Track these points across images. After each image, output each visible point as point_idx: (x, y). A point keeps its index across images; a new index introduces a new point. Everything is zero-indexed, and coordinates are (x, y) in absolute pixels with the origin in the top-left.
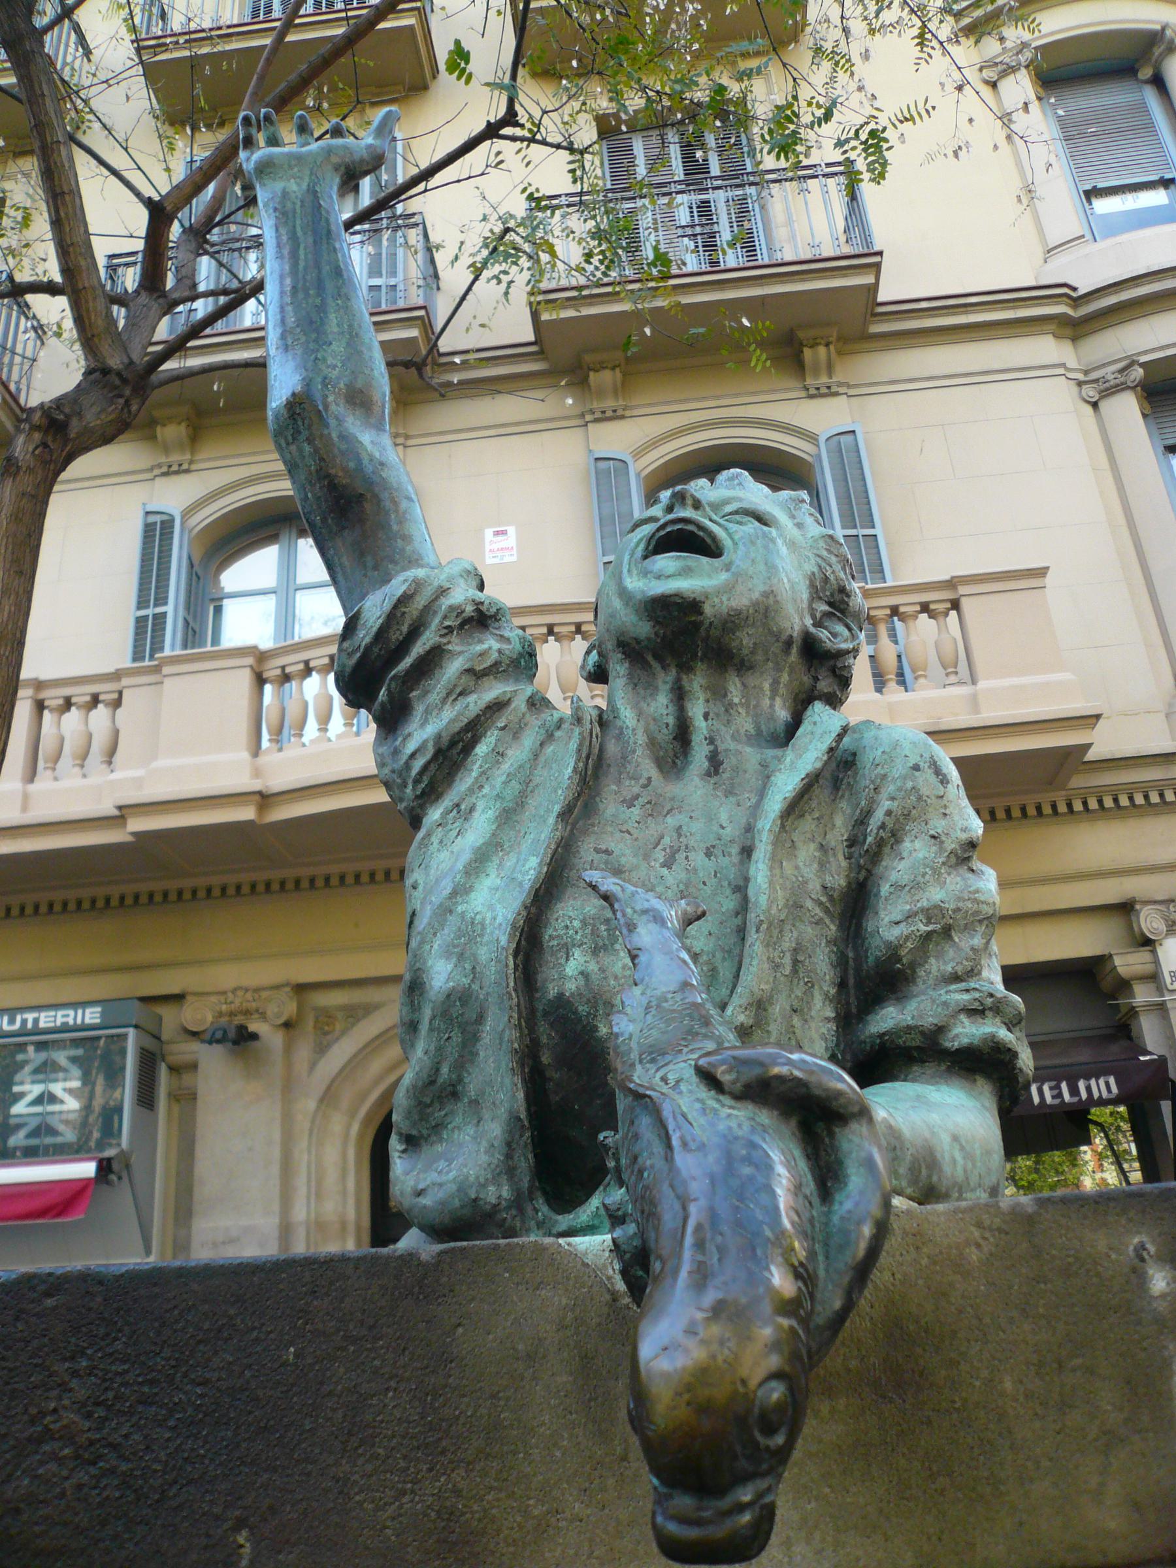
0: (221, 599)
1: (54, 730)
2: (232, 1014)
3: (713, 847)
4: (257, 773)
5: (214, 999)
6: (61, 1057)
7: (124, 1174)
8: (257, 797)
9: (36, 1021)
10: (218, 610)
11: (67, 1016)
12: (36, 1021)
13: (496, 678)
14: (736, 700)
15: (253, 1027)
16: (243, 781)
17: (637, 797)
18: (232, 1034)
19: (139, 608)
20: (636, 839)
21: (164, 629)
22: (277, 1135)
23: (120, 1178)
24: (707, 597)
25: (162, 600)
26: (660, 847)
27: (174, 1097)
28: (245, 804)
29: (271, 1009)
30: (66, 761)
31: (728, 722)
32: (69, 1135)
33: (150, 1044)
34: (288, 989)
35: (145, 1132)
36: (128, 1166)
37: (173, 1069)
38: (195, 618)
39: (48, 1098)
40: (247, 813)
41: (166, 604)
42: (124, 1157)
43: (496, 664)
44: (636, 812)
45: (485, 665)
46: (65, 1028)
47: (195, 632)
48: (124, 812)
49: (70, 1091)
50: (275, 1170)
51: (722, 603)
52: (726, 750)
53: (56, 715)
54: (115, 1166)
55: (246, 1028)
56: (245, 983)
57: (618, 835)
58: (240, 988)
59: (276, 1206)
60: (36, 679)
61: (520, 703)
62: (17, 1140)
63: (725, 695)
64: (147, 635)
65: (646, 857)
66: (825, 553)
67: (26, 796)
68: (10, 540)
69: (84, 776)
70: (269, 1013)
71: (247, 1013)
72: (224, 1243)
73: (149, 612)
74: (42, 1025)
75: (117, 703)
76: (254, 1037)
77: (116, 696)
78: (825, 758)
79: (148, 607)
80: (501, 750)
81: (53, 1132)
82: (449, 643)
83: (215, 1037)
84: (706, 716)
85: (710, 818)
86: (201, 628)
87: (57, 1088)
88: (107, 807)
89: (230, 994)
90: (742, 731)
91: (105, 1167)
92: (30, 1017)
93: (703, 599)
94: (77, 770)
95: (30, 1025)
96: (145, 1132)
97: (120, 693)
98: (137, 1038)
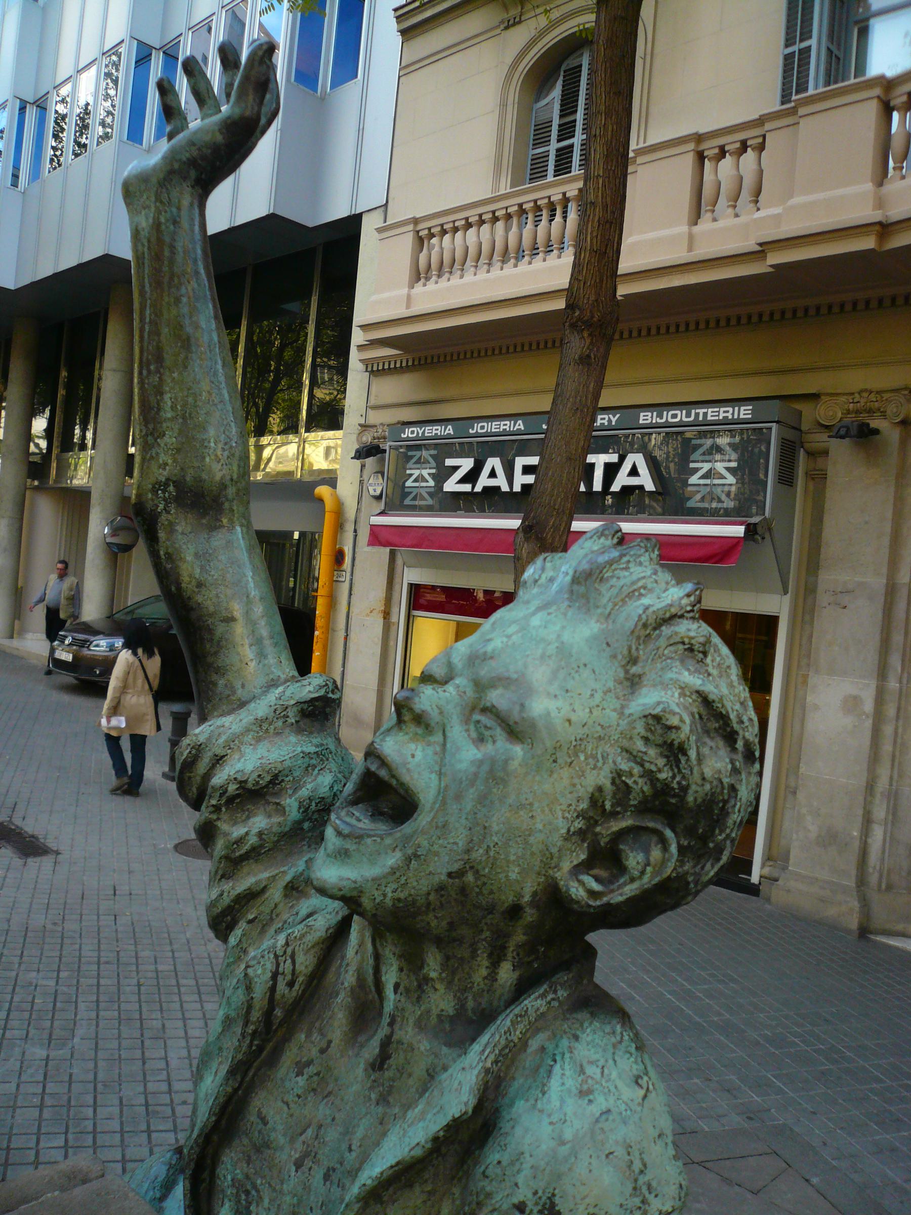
0: (868, 19)
1: (712, 177)
2: (858, 412)
3: (334, 1170)
4: (880, 203)
5: (843, 399)
7: (767, 536)
8: (877, 228)
9: (705, 414)
10: (864, 32)
11: (728, 412)
12: (705, 414)
13: (256, 861)
14: (433, 975)
15: (874, 424)
16: (866, 213)
17: (309, 1063)
18: (854, 431)
19: (787, 46)
20: (292, 1116)
21: (809, 63)
22: (889, 515)
23: (763, 538)
24: (361, 892)
25: (806, 35)
26: (303, 1137)
27: (810, 476)
28: (867, 234)
29: (891, 409)
30: (722, 201)
31: (419, 999)
32: (729, 504)
33: (790, 435)
34: (906, 392)
35: (785, 506)
36: (770, 529)
37: (810, 454)
38: (839, 45)
40: (868, 243)
41: (810, 37)
42: (767, 525)
43: (254, 849)
44: (301, 1081)
45: (242, 852)
47: (838, 58)
48: (765, 248)
49: (727, 469)
50: (886, 541)
51: (385, 895)
52: (400, 1042)
53: (713, 163)
54: (759, 529)
55: (868, 424)
56: (868, 387)
57: (280, 1104)
58: (866, 390)
59: (884, 570)
60: (696, 134)
61: (276, 894)
63: (421, 967)
64: (794, 70)
65: (292, 1140)
66: (640, 745)
67: (691, 237)
68: (608, 65)
69: (737, 216)
70: (889, 413)
71: (870, 411)
72: (841, 592)
73: (795, 48)
74: (709, 418)
75: (761, 147)
76: (876, 432)
77: (760, 140)
78: (429, 1146)
79: (794, 43)
80: (245, 946)
82: (218, 819)
83: (840, 432)
84: (396, 987)
85: (347, 1132)
86: (845, 56)
87: (720, 467)
88: (750, 245)
89: (857, 395)
90: (435, 1011)
91: (751, 530)
92: (701, 411)
93: (355, 894)
94: (730, 210)
95: (701, 418)
96: (785, 506)
97: (764, 137)
98: (779, 431)
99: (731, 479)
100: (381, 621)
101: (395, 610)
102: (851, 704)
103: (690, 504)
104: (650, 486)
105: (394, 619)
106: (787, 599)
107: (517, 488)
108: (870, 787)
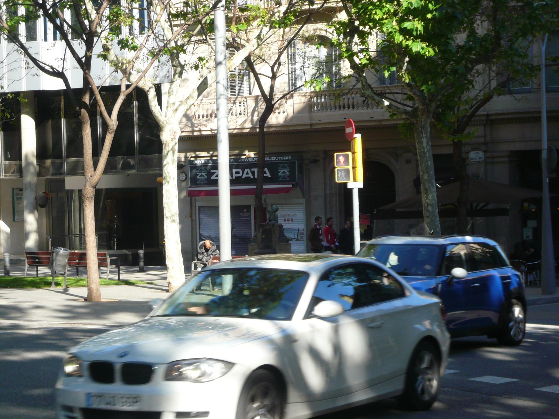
6: (285, 165)
32: (288, 179)
40: (309, 127)
46: (285, 160)
62: (280, 179)
76: (319, 160)
81: (285, 178)
87: (285, 171)
91: (293, 186)
99: (288, 173)
100: (190, 219)
101: (194, 216)
103: (280, 179)
104: (270, 176)
105: (194, 218)
107: (234, 178)
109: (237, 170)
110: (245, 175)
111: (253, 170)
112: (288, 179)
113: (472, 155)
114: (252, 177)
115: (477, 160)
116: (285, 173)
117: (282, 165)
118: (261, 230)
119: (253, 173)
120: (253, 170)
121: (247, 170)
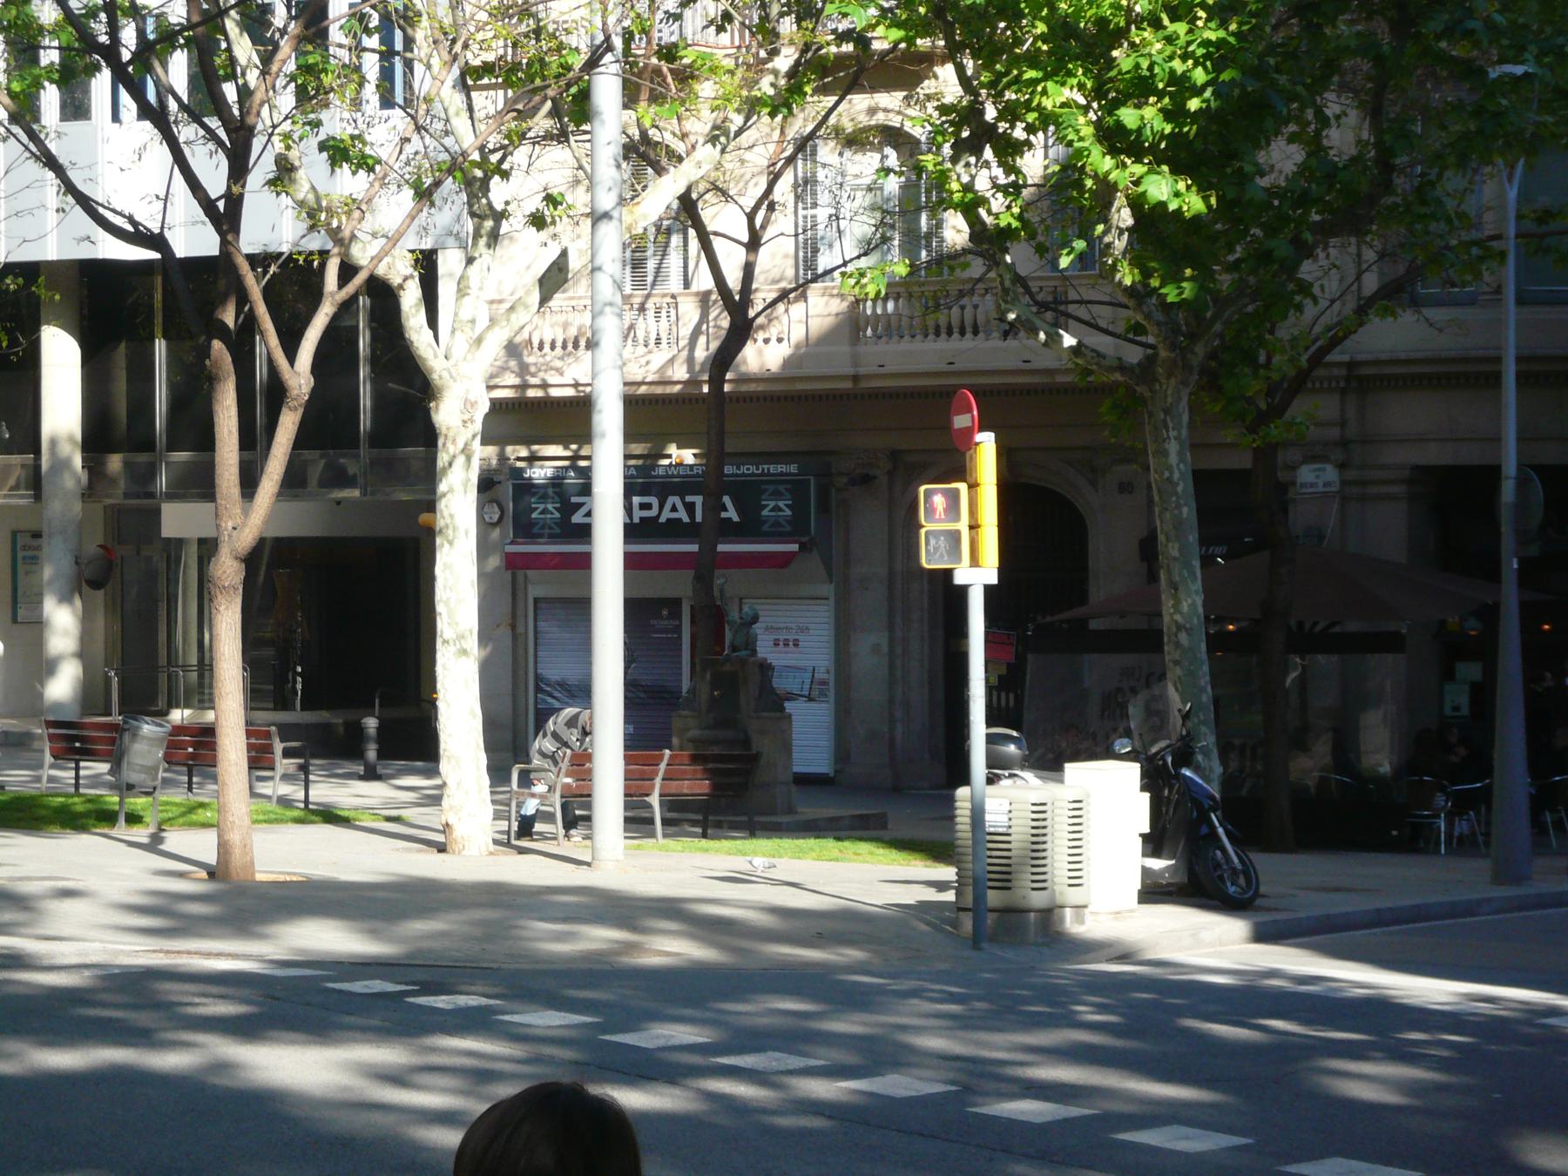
6: (781, 488)
32: (788, 528)
39: (777, 509)
40: (848, 385)
46: (782, 474)
62: (765, 528)
87: (781, 504)
91: (803, 546)
99: (788, 512)
100: (508, 632)
102: (876, 649)
103: (765, 528)
104: (736, 518)
105: (520, 629)
106: (832, 587)
107: (636, 520)
108: (891, 701)
109: (646, 499)
110: (666, 515)
111: (689, 499)
112: (788, 528)
113: (1306, 474)
114: (686, 519)
115: (1321, 489)
116: (780, 510)
117: (771, 488)
118: (708, 676)
119: (690, 508)
120: (689, 499)
121: (676, 500)
